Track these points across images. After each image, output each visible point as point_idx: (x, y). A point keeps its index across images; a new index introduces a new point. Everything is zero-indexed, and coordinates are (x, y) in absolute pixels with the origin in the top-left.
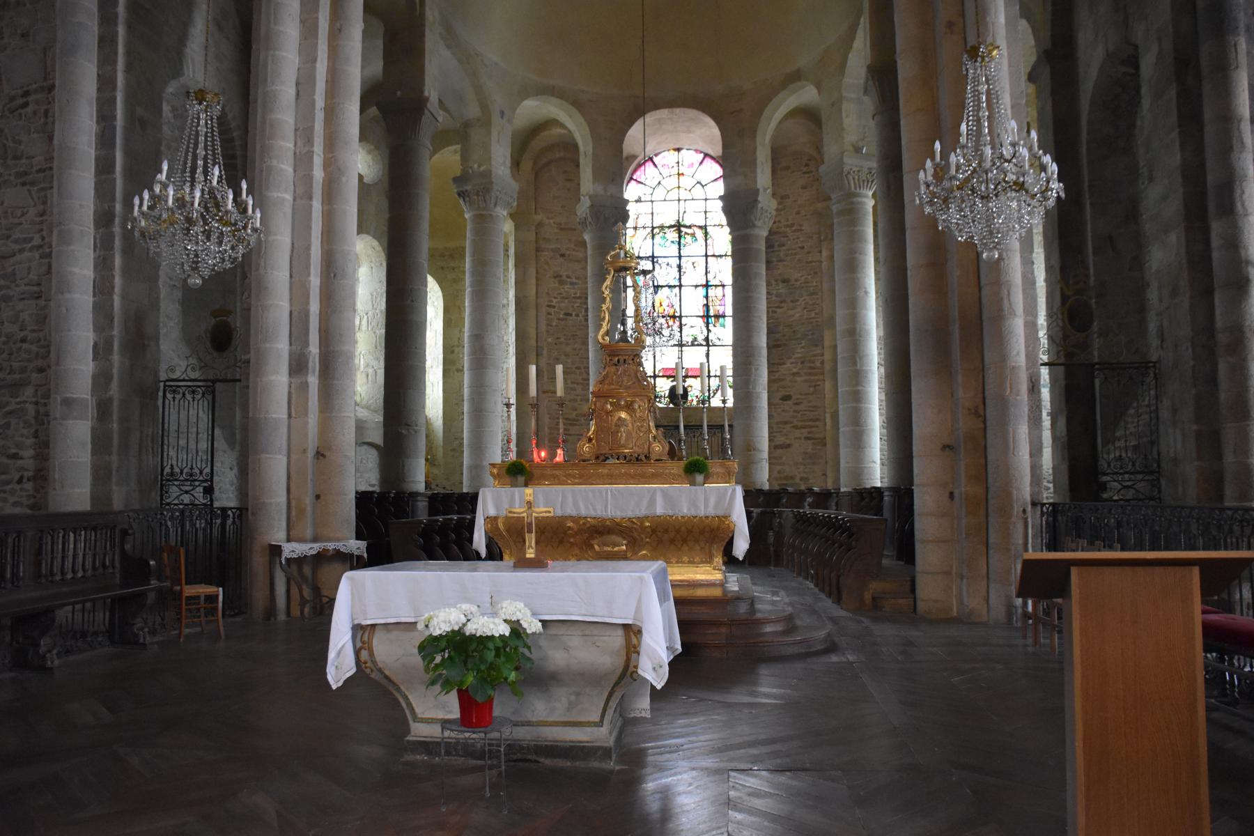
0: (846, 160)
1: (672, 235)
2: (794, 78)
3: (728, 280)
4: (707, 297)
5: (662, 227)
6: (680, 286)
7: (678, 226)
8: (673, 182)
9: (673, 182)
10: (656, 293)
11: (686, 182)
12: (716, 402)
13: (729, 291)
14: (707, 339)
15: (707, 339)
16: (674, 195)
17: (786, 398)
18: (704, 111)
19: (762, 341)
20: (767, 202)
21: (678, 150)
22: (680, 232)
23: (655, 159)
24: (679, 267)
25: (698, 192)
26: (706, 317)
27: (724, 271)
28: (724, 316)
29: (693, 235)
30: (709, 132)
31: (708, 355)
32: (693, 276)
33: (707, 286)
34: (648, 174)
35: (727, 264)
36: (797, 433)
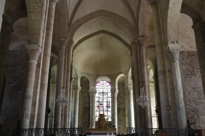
0: (129, 86)
1: (102, 94)
2: (121, 73)
3: (111, 101)
4: (107, 104)
5: (100, 93)
6: (103, 102)
7: (103, 92)
8: (102, 86)
9: (102, 86)
10: (99, 103)
11: (104, 86)
12: (109, 120)
13: (111, 103)
14: (107, 110)
15: (107, 110)
16: (102, 88)
17: (120, 120)
18: (108, 77)
19: (116, 111)
20: (117, 91)
21: (103, 81)
22: (103, 93)
23: (100, 82)
24: (103, 99)
25: (106, 87)
26: (107, 107)
27: (110, 100)
28: (110, 107)
29: (105, 94)
30: (109, 80)
31: (107, 113)
32: (105, 100)
33: (107, 102)
34: (98, 84)
35: (110, 99)
36: (121, 126)
